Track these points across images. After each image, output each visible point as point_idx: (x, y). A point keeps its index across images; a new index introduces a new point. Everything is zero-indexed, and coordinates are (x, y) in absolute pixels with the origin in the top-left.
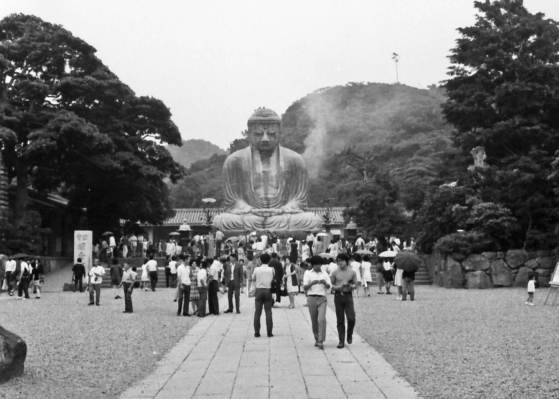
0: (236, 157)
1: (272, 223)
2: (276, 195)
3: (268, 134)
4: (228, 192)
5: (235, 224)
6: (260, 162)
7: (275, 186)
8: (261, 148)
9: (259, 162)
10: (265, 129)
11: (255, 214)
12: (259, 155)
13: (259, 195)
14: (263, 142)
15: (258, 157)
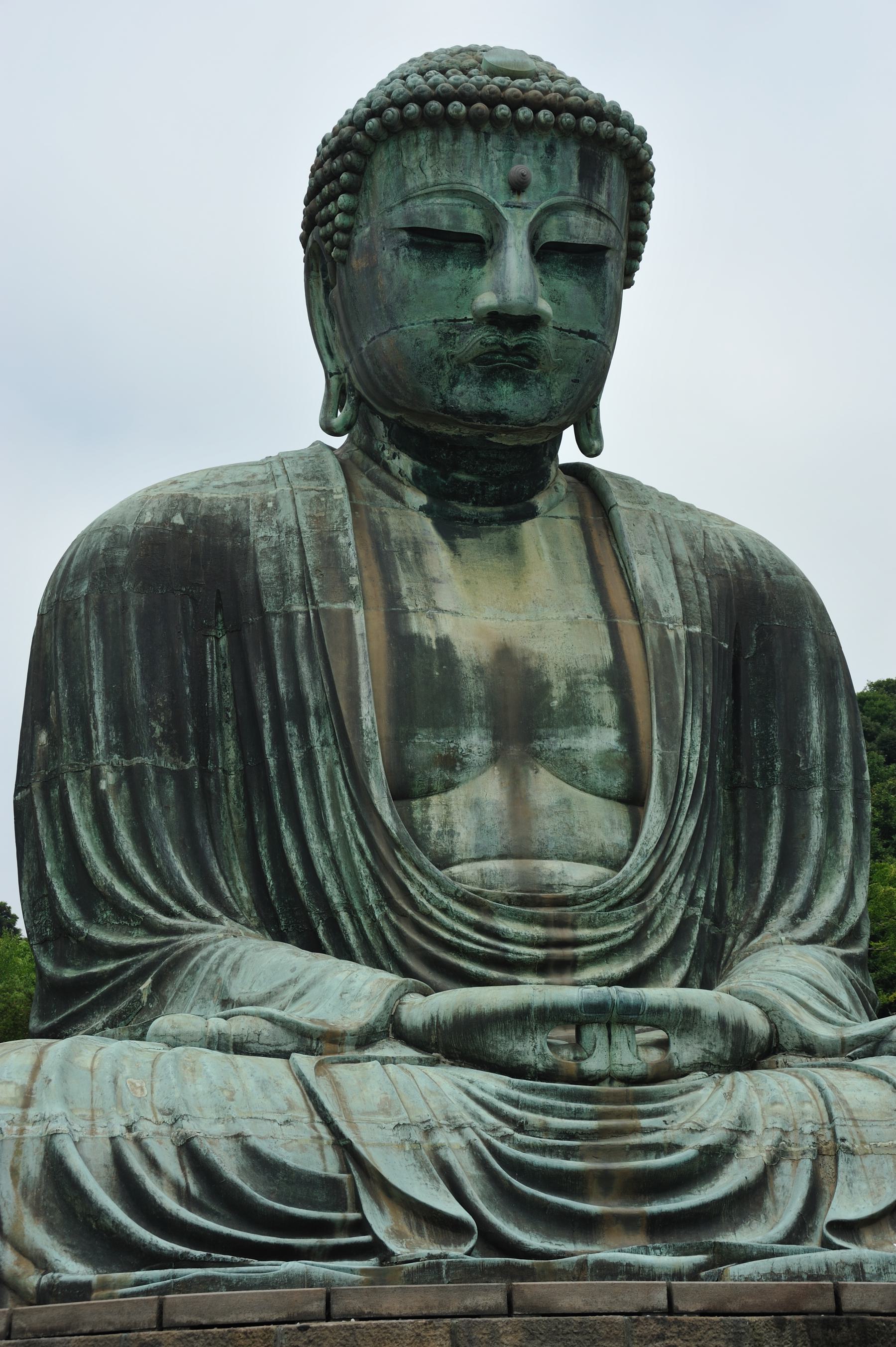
0: (180, 502)
1: (712, 1160)
2: (636, 868)
3: (543, 253)
4: (88, 841)
5: (230, 1166)
6: (439, 557)
7: (617, 783)
8: (467, 395)
9: (418, 548)
10: (518, 187)
11: (457, 1043)
12: (417, 499)
13: (444, 861)
14: (497, 318)
15: (410, 515)
